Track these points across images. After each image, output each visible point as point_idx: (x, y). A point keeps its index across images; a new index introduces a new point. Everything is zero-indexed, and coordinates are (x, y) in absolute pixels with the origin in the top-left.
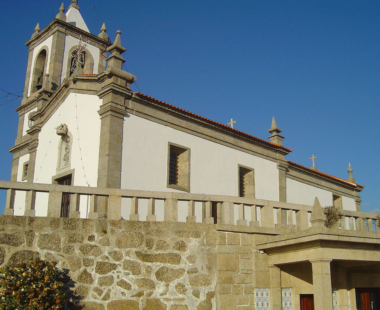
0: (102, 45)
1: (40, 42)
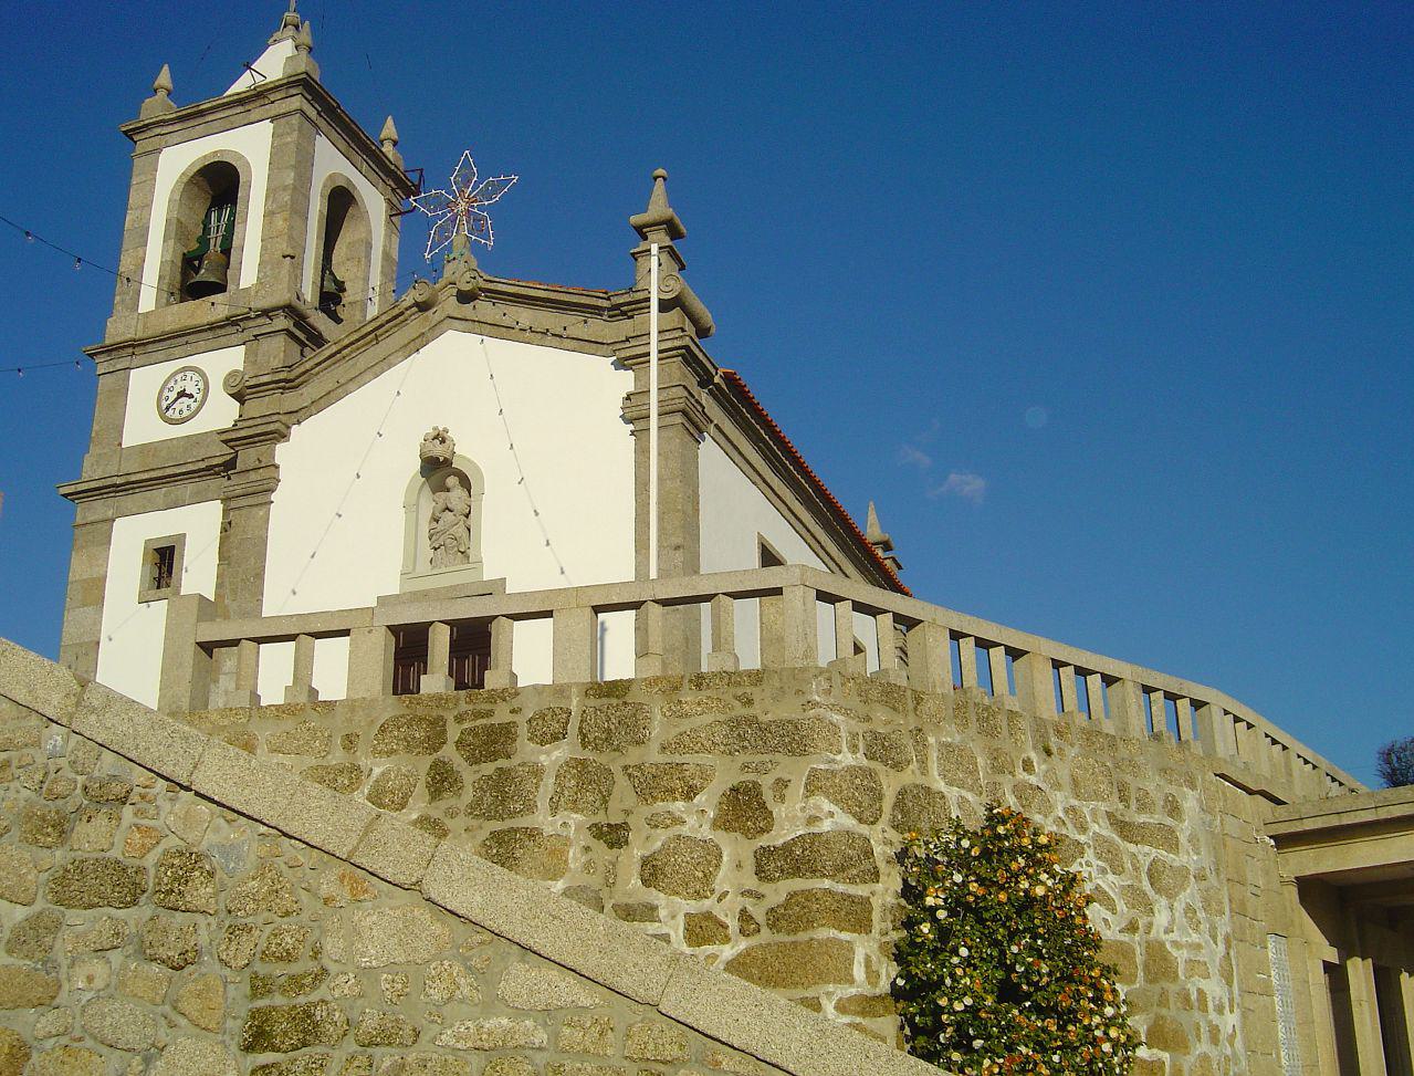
0: (393, 190)
1: (194, 133)
